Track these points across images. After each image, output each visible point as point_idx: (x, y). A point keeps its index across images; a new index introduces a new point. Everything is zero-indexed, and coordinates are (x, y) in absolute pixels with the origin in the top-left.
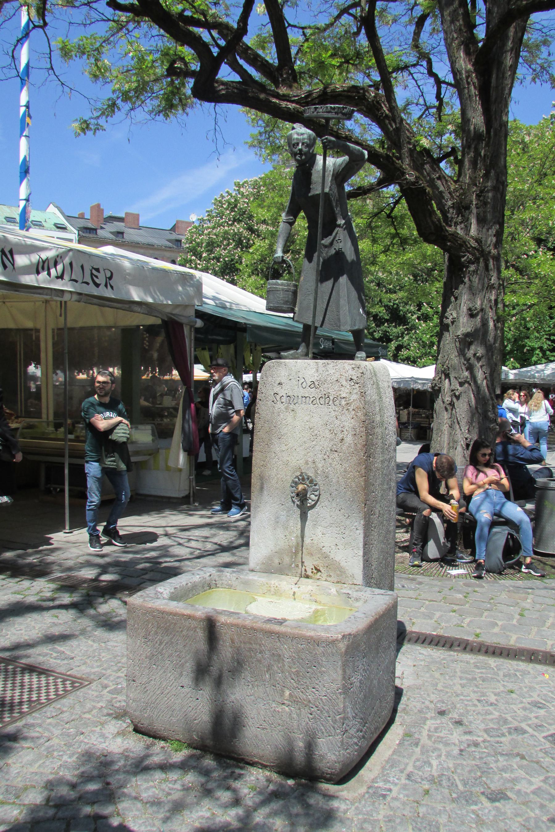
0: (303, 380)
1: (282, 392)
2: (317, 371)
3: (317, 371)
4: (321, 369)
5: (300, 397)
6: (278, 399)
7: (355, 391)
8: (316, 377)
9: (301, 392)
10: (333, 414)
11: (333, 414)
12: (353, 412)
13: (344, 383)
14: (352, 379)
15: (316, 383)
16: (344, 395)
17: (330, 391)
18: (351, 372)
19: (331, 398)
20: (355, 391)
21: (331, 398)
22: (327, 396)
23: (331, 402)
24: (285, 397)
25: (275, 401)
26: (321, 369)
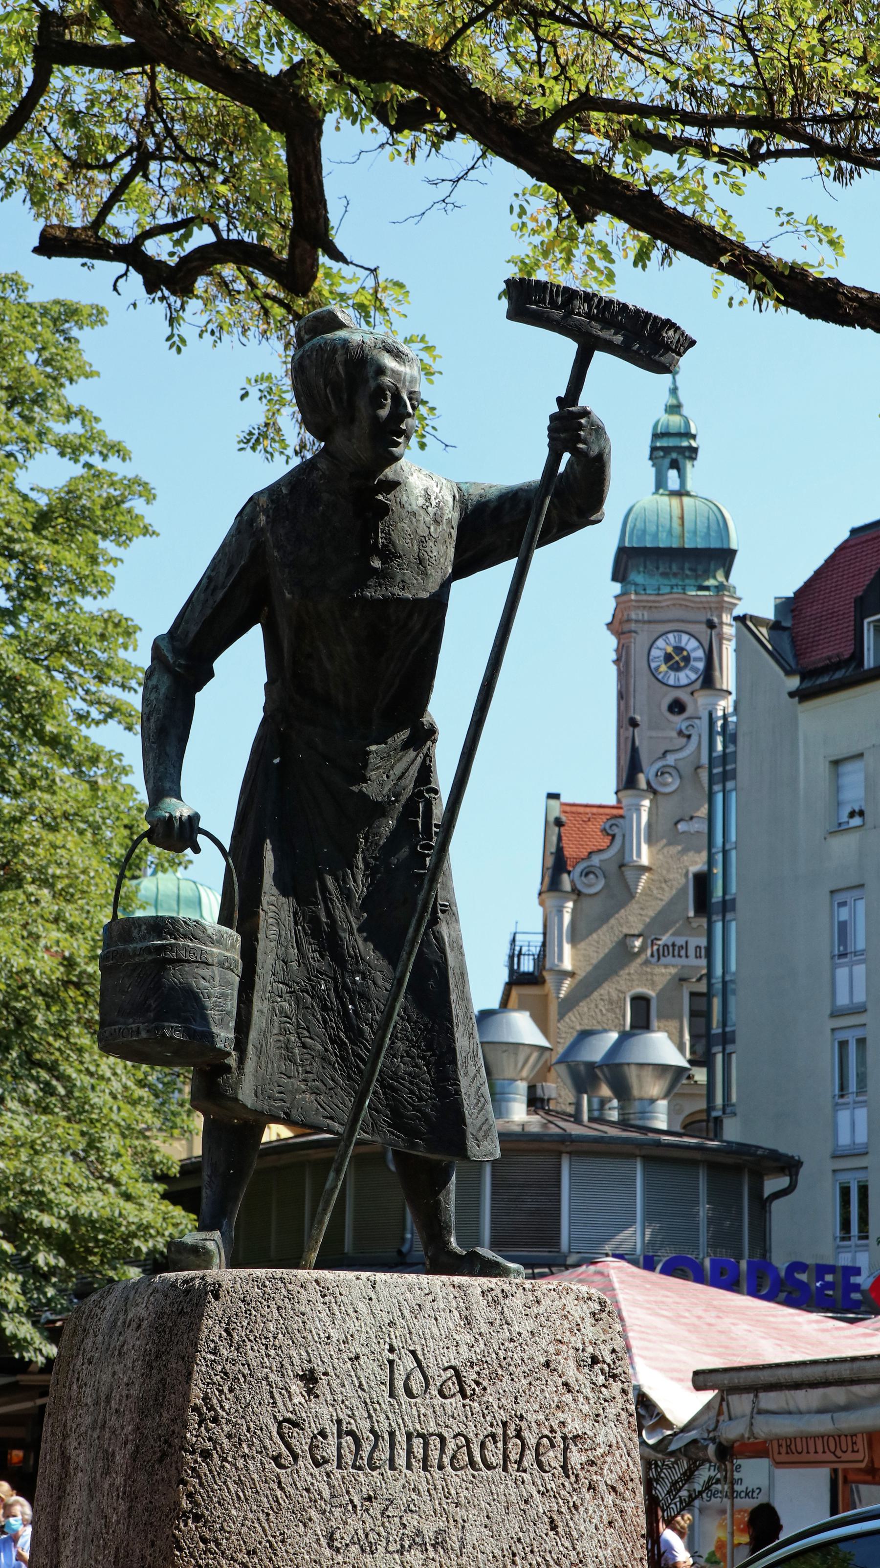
0: (410, 1363)
1: (321, 1413)
2: (468, 1322)
3: (468, 1322)
4: (481, 1310)
5: (401, 1438)
6: (301, 1444)
7: (612, 1410)
8: (463, 1349)
9: (415, 1414)
10: (540, 1505)
11: (540, 1505)
12: (610, 1499)
13: (571, 1372)
14: (595, 1360)
15: (470, 1376)
16: (575, 1426)
17: (520, 1409)
18: (589, 1331)
19: (532, 1441)
20: (612, 1410)
21: (532, 1441)
22: (511, 1431)
23: (529, 1458)
24: (332, 1440)
25: (287, 1459)
26: (481, 1310)
